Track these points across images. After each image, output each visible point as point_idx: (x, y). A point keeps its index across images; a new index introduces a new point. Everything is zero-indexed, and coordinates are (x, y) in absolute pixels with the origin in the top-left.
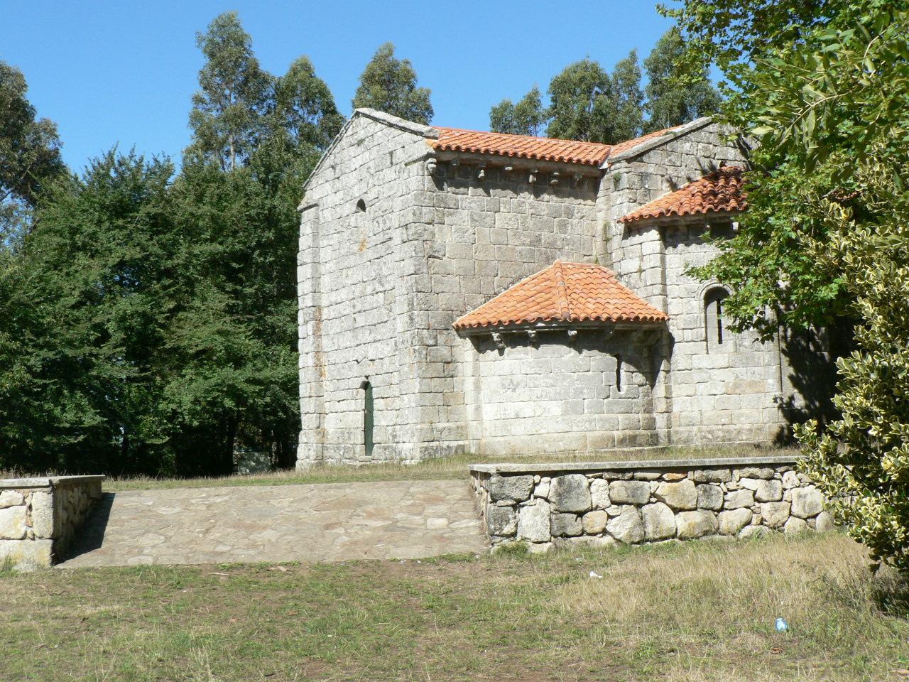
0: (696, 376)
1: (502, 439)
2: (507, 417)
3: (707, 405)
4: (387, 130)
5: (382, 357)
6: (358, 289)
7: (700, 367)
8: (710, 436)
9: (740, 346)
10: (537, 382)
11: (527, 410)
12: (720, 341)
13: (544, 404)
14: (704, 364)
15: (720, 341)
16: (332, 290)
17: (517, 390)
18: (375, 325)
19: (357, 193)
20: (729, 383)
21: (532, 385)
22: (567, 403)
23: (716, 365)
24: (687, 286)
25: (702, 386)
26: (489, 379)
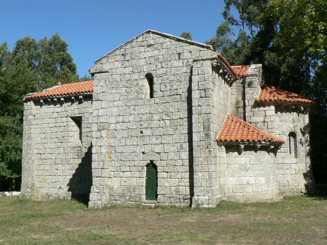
0: (286, 167)
1: (242, 194)
2: (243, 184)
3: (289, 178)
4: (174, 42)
5: (167, 152)
6: (145, 117)
7: (287, 163)
8: (292, 191)
9: (300, 155)
10: (256, 168)
11: (253, 181)
12: (290, 153)
13: (259, 178)
14: (288, 162)
15: (290, 153)
16: (119, 115)
17: (248, 171)
18: (161, 136)
19: (146, 69)
20: (297, 170)
21: (254, 169)
22: (267, 178)
23: (293, 163)
24: (283, 130)
25: (288, 170)
26: (232, 166)
